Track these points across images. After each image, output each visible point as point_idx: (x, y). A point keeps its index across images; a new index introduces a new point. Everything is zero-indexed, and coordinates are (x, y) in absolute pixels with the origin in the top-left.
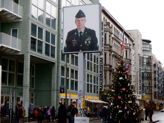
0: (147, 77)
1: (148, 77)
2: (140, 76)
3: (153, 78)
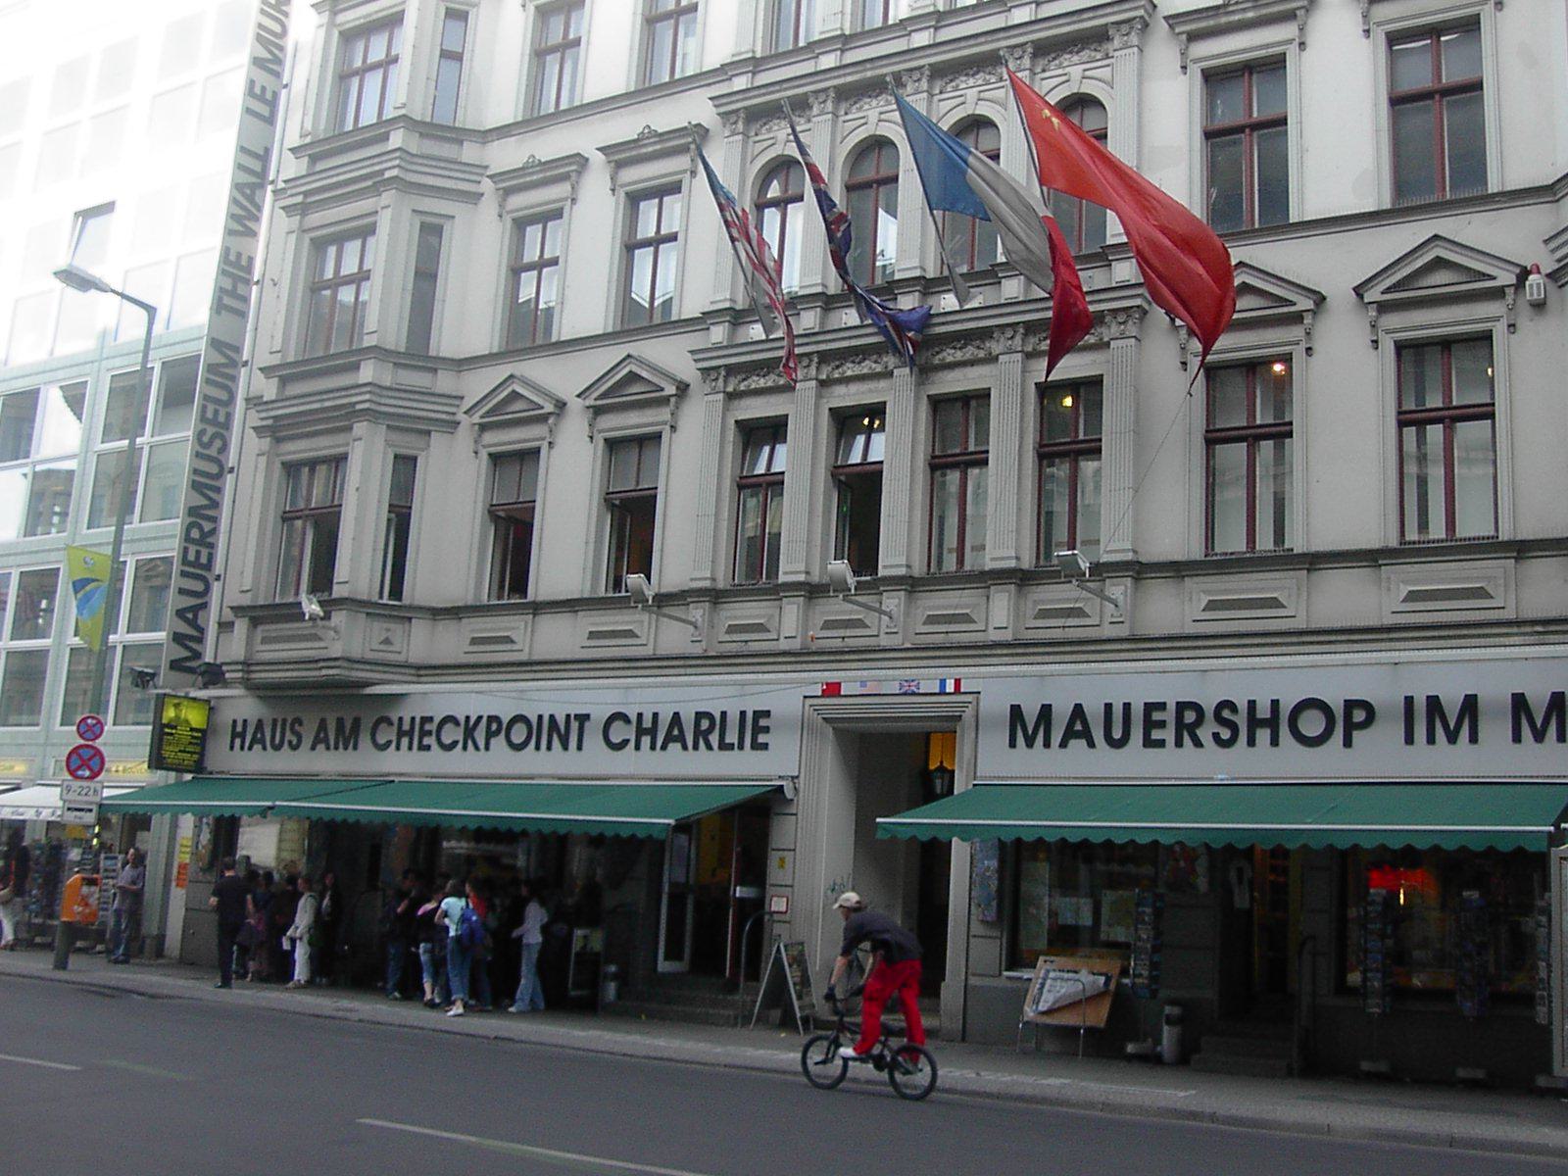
2: (480, 735)
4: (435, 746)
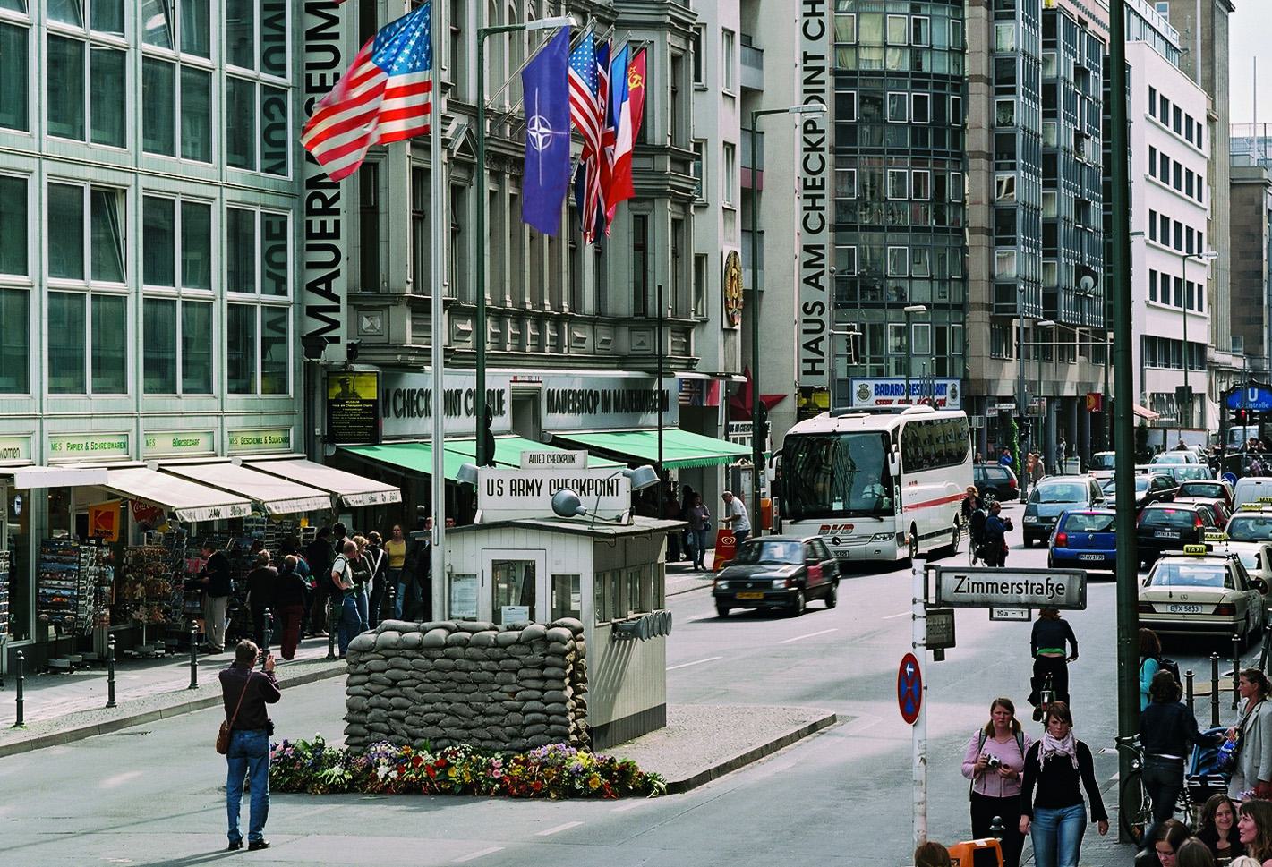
0: (915, 129)
1: (924, 129)
2: (814, 138)
3: (977, 139)
4: (821, 176)
